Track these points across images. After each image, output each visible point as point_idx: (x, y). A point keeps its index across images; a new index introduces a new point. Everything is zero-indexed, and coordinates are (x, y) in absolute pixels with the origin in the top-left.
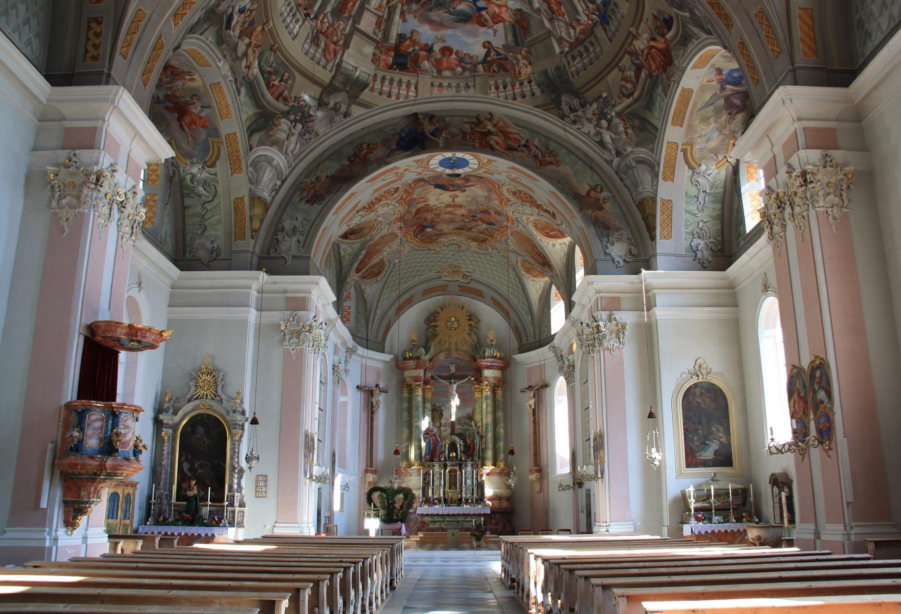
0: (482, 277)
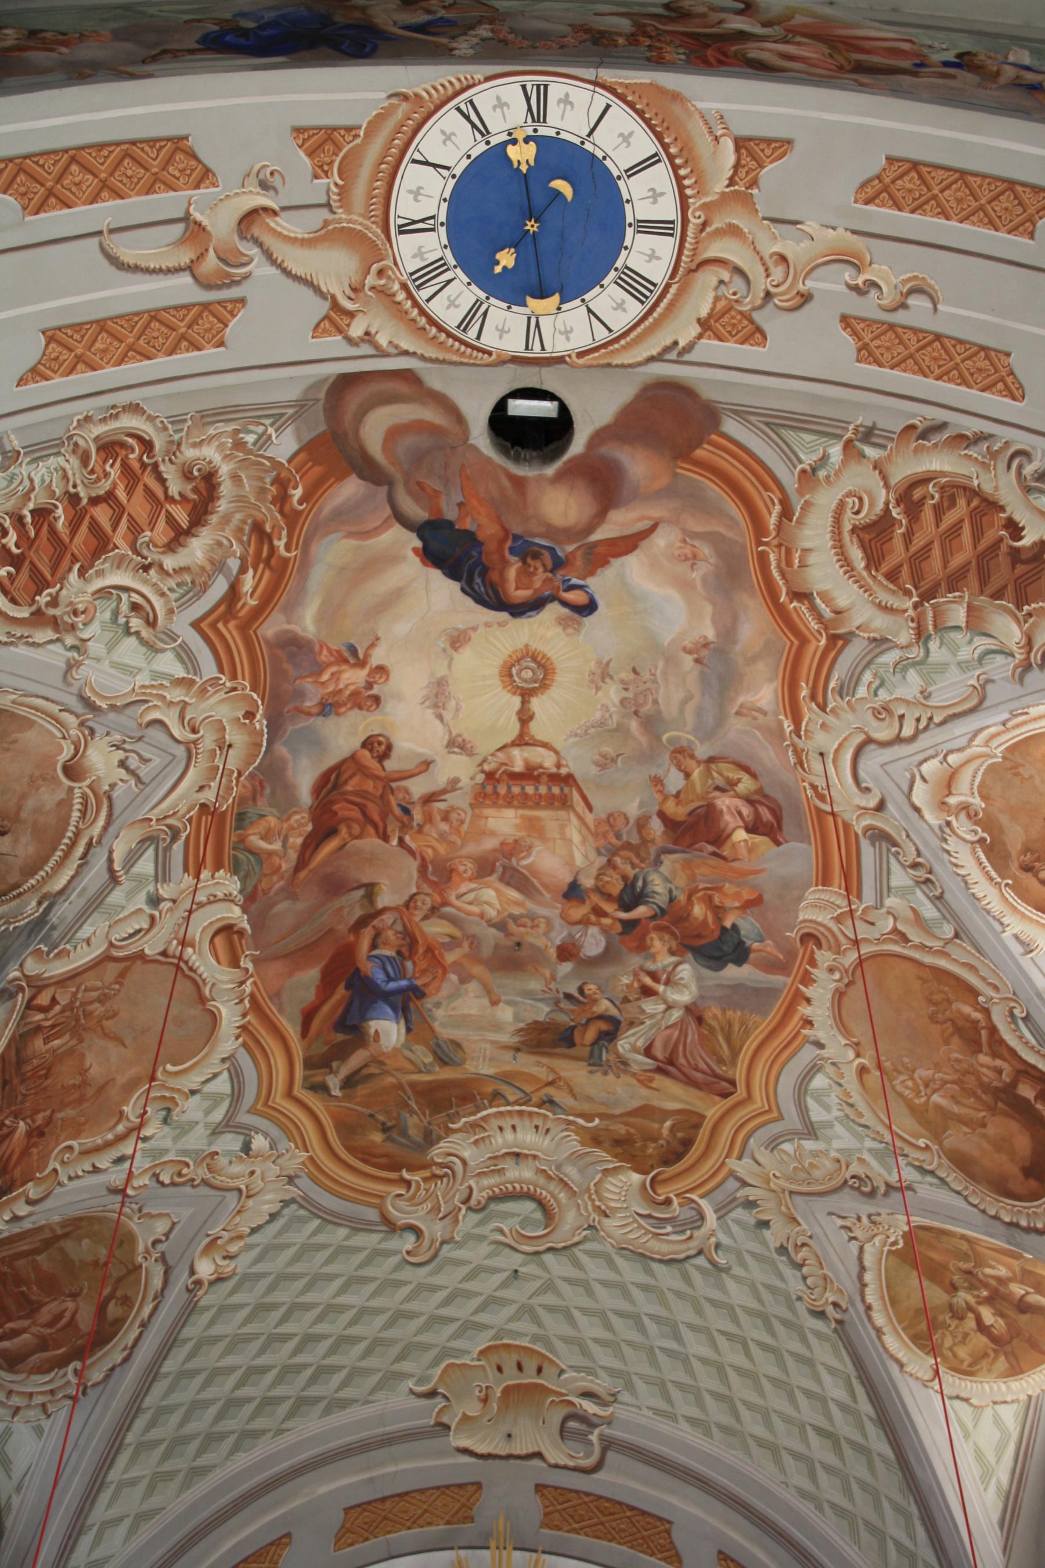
0: (664, 1426)
